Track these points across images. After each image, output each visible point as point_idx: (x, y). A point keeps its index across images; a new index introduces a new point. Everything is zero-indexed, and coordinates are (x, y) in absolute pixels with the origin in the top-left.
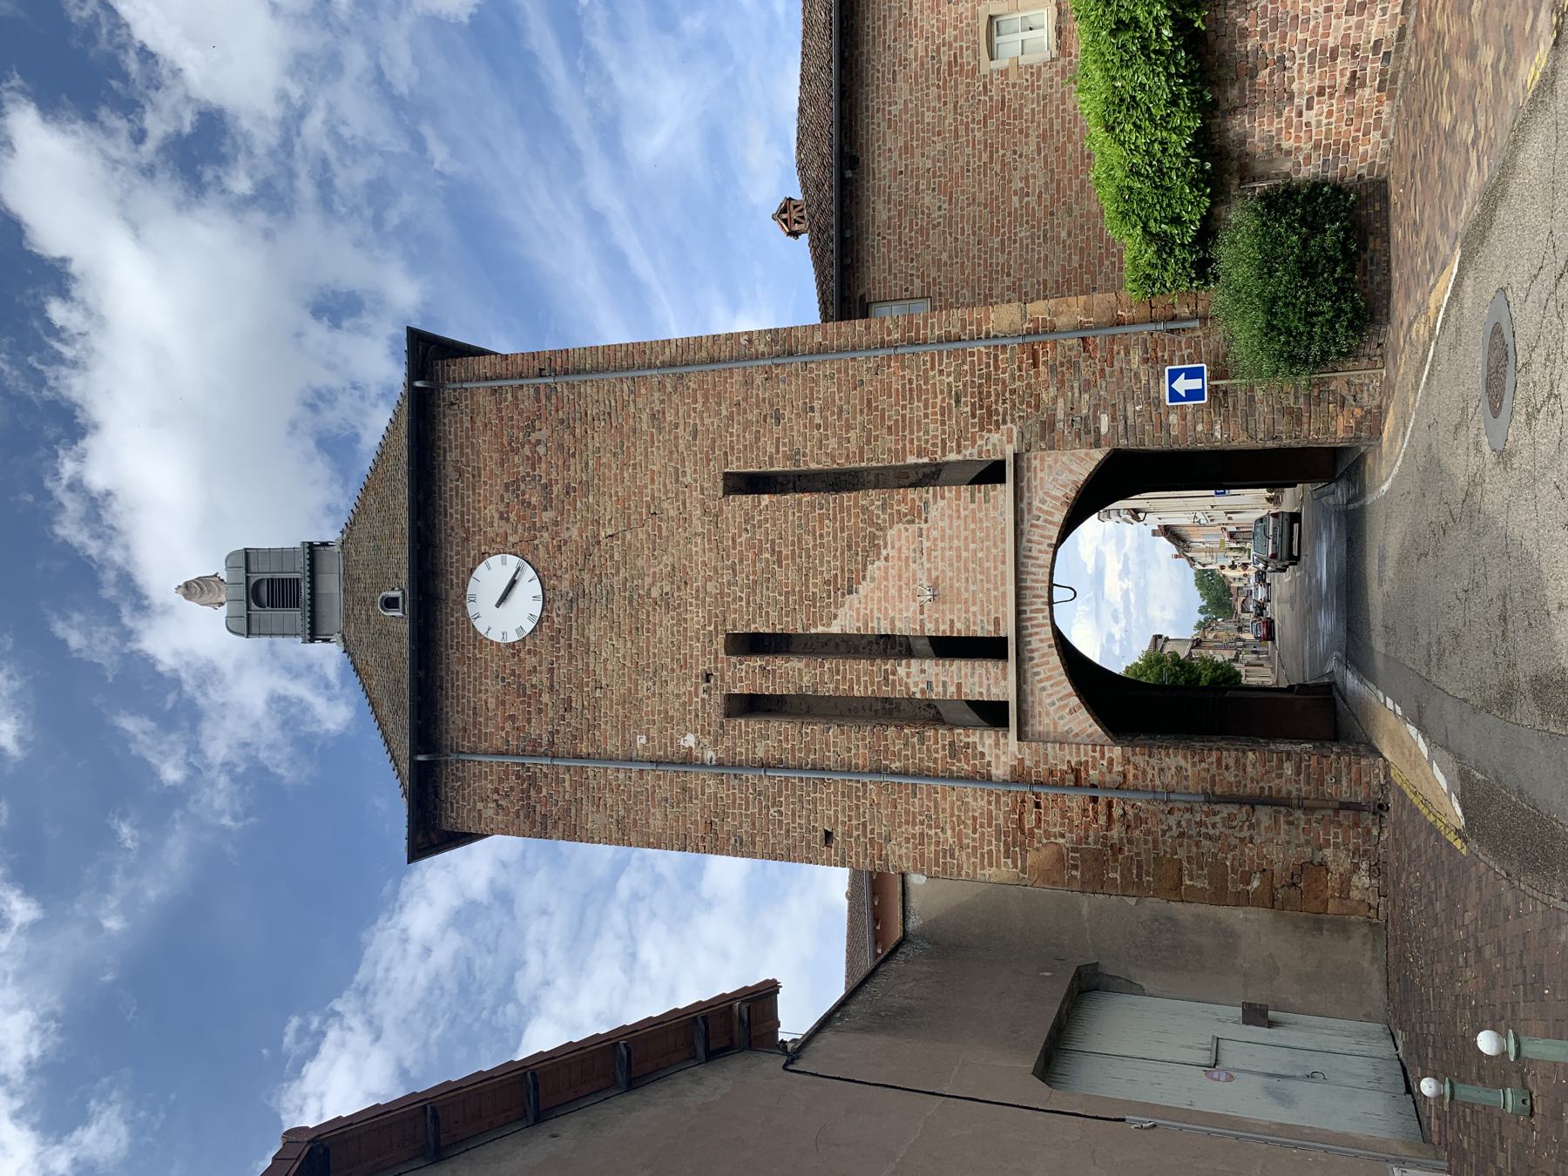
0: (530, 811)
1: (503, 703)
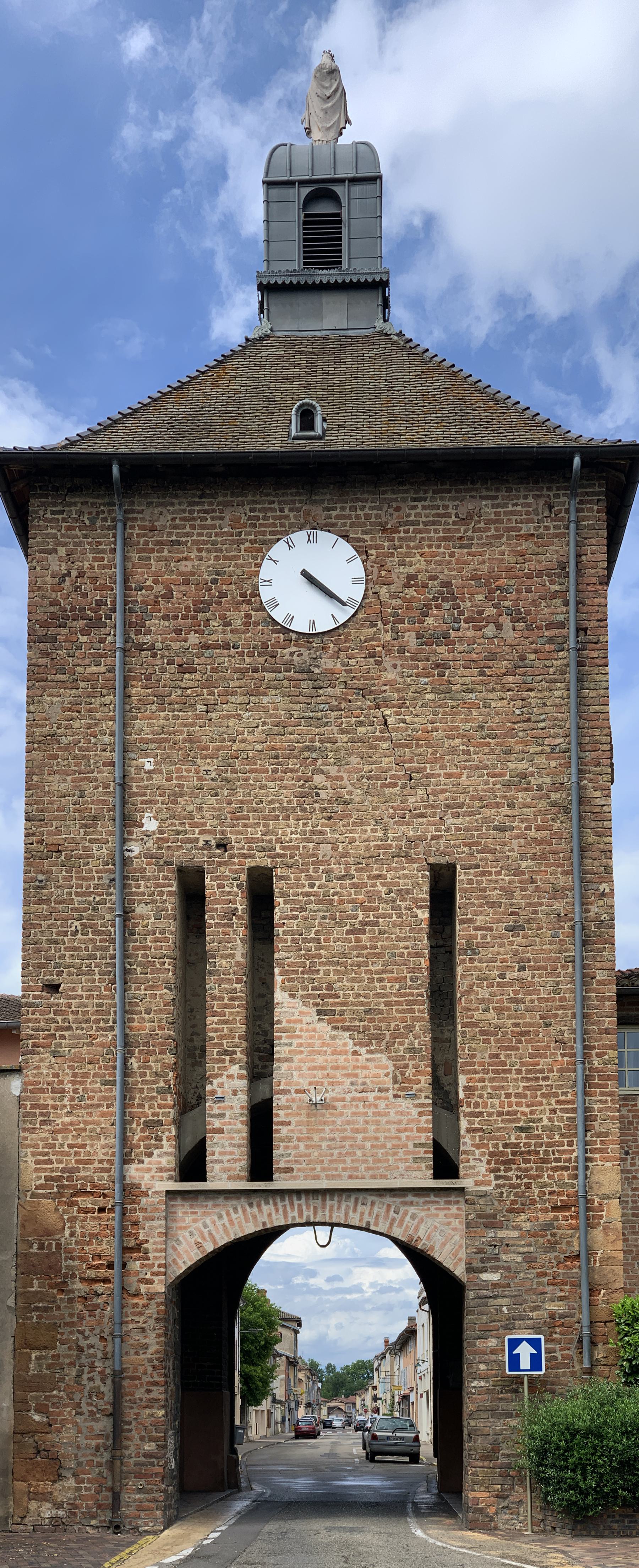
0: (60, 619)
1: (186, 582)
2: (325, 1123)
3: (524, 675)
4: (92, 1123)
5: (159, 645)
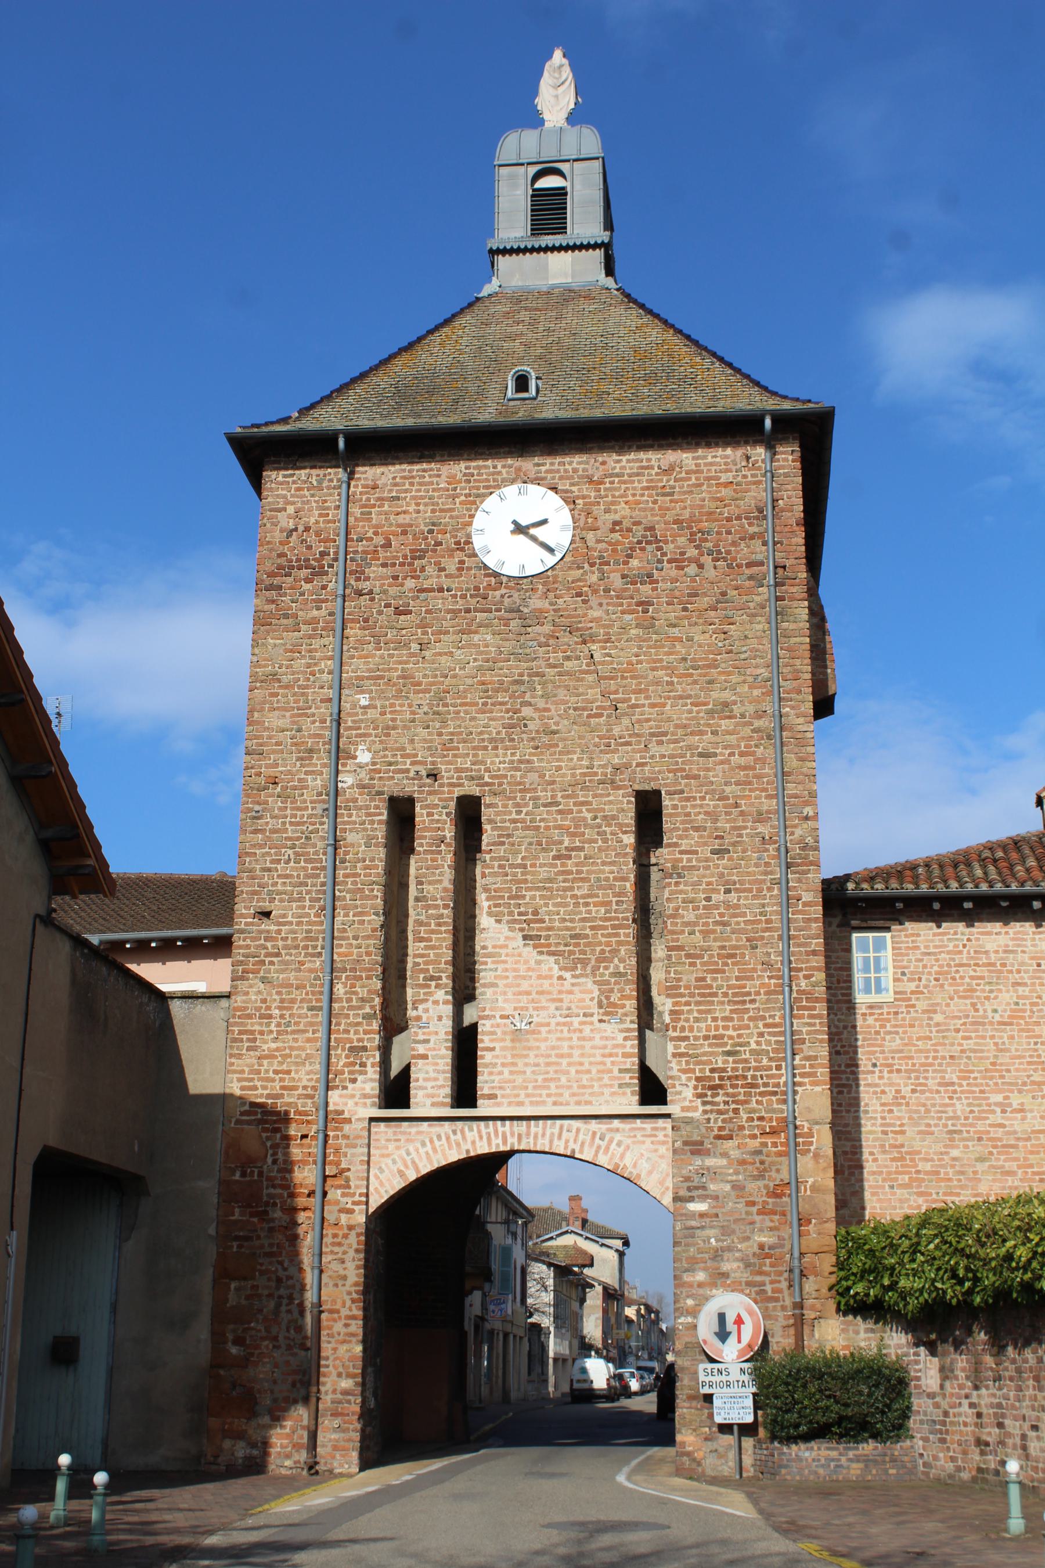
0: (286, 570)
1: (404, 533)
2: (530, 1048)
3: (725, 609)
4: (299, 1048)
5: (377, 590)
